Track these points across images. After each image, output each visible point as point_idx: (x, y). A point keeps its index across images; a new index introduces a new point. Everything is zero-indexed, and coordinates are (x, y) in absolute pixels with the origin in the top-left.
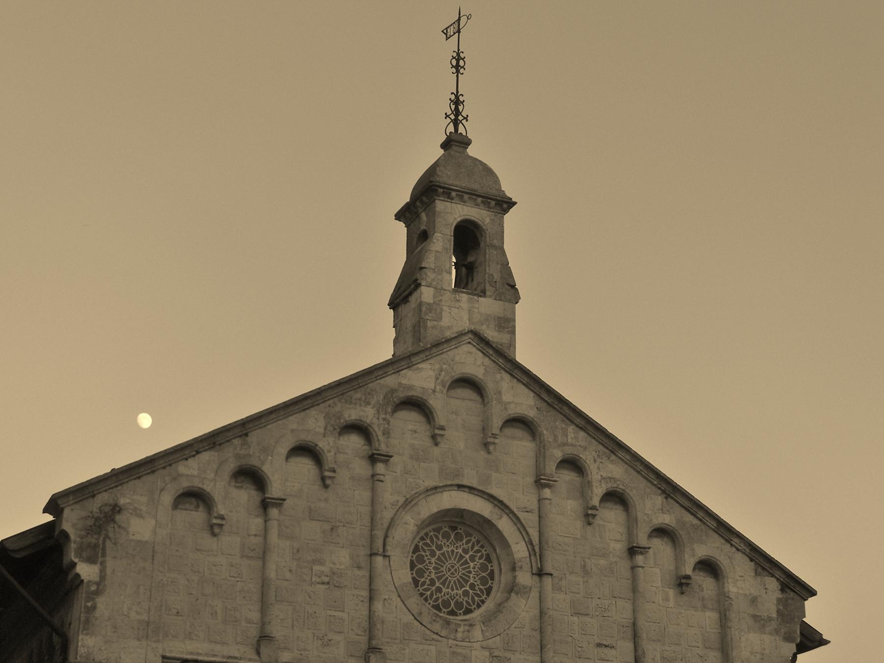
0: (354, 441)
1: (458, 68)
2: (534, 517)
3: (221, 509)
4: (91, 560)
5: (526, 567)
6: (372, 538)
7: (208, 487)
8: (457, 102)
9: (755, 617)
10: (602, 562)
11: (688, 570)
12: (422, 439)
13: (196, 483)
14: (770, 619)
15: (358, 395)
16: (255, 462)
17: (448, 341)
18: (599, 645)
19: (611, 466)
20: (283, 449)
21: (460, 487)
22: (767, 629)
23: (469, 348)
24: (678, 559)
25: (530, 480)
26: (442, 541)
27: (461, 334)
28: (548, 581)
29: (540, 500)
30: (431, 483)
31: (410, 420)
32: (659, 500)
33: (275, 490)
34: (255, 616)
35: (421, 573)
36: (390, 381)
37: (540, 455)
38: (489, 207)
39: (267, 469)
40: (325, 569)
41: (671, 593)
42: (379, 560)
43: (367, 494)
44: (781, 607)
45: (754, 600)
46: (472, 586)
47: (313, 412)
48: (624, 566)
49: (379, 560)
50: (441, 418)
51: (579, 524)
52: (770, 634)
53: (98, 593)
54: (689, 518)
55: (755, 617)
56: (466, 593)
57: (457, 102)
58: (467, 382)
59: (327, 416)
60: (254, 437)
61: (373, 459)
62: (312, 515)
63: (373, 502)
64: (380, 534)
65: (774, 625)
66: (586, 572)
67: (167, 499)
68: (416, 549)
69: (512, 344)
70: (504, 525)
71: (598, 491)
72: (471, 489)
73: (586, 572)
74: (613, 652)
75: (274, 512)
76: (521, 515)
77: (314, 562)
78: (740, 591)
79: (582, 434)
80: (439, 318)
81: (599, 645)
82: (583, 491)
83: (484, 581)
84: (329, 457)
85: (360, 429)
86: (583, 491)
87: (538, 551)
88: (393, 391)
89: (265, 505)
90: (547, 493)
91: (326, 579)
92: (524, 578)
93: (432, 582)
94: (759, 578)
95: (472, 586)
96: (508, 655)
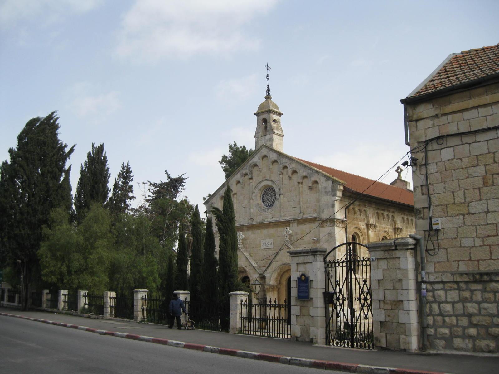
1: (268, 79)
8: (268, 87)
9: (326, 192)
10: (294, 188)
11: (310, 185)
14: (329, 192)
15: (245, 167)
18: (293, 208)
21: (265, 180)
22: (329, 194)
26: (268, 192)
27: (261, 147)
32: (303, 169)
35: (264, 200)
38: (266, 114)
40: (244, 205)
41: (309, 191)
42: (252, 201)
45: (325, 188)
46: (273, 200)
52: (329, 195)
54: (310, 172)
55: (326, 192)
57: (268, 87)
58: (265, 156)
65: (330, 193)
66: (290, 191)
71: (290, 172)
74: (296, 208)
81: (293, 208)
88: (251, 164)
93: (266, 201)
94: (327, 182)
96: (275, 214)
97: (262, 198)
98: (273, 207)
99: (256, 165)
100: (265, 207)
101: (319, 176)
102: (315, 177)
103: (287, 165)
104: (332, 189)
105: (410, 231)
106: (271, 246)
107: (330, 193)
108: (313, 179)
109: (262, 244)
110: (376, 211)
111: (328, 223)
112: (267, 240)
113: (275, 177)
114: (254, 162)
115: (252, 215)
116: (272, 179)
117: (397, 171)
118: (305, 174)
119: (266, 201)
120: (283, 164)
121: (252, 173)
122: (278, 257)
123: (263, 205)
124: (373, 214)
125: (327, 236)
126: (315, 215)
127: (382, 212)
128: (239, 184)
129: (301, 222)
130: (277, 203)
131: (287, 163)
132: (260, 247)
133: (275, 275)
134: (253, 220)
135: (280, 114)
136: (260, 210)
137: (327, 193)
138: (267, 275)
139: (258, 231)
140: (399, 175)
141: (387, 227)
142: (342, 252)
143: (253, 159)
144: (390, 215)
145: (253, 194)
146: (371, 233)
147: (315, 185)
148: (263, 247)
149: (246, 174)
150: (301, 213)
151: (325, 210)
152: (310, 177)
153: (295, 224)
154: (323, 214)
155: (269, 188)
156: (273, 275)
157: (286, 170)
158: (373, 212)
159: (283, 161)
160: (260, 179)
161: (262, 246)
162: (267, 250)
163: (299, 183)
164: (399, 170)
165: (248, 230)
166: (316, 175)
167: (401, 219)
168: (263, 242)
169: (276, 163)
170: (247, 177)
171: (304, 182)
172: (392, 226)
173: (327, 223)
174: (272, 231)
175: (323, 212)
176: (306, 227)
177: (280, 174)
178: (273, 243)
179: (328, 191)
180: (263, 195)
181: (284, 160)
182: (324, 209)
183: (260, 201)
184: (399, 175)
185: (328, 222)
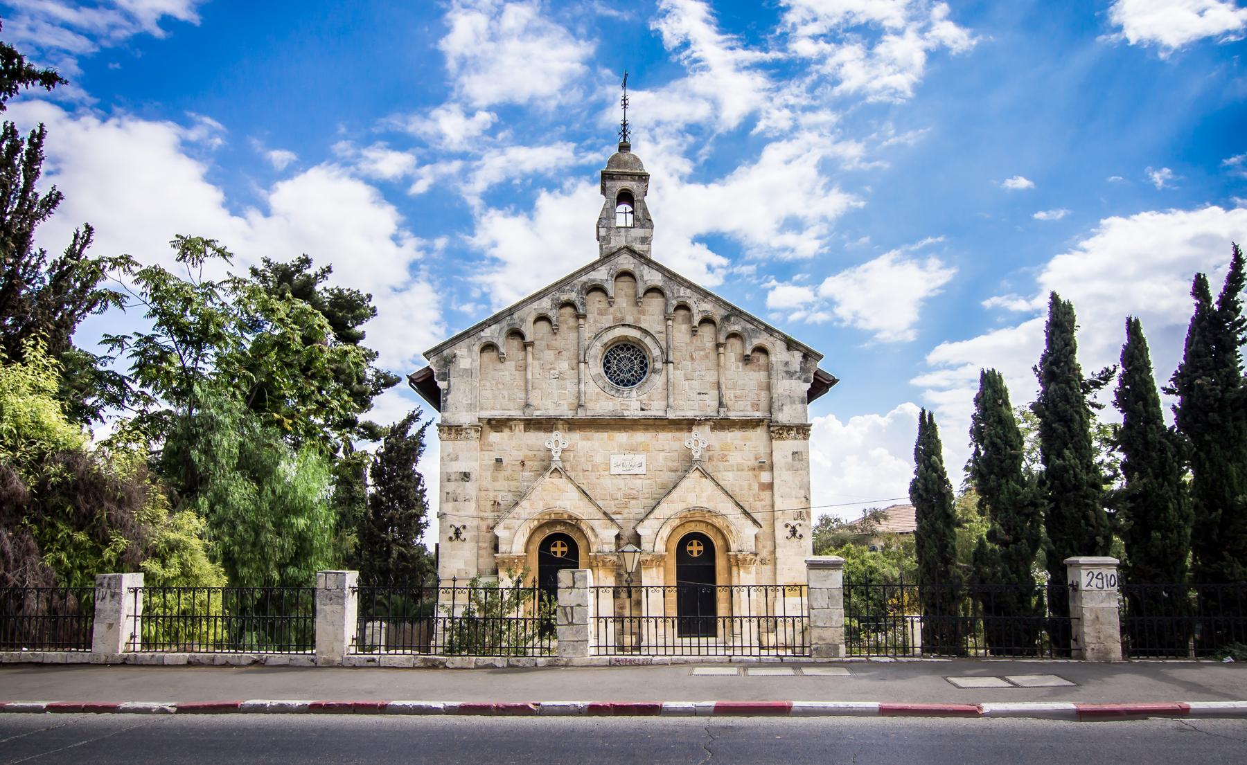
0: (568, 310)
2: (664, 335)
3: (502, 350)
4: (444, 380)
5: (660, 359)
6: (579, 355)
7: (495, 341)
10: (702, 353)
11: (748, 352)
12: (604, 305)
13: (489, 339)
14: (796, 372)
16: (517, 327)
17: (613, 254)
19: (705, 305)
20: (531, 319)
21: (623, 325)
23: (626, 256)
24: (744, 347)
25: (662, 317)
27: (620, 250)
28: (671, 365)
29: (667, 327)
30: (607, 326)
31: (596, 297)
33: (528, 339)
34: (523, 396)
36: (584, 278)
37: (666, 305)
39: (523, 329)
41: (740, 364)
42: (582, 365)
43: (576, 334)
45: (787, 364)
46: (636, 372)
47: (545, 299)
48: (713, 356)
49: (582, 365)
50: (611, 294)
51: (689, 336)
53: (447, 393)
54: (749, 326)
55: (787, 372)
56: (632, 375)
58: (626, 274)
59: (552, 300)
60: (516, 316)
61: (578, 317)
62: (549, 347)
63: (578, 338)
64: (582, 353)
66: (692, 359)
67: (477, 349)
68: (606, 357)
69: (649, 250)
70: (648, 341)
71: (697, 319)
72: (629, 326)
73: (692, 359)
75: (529, 349)
76: (657, 336)
77: (551, 369)
79: (688, 291)
80: (609, 243)
82: (690, 319)
83: (642, 368)
84: (554, 319)
85: (569, 304)
86: (690, 319)
87: (665, 352)
88: (585, 283)
89: (525, 346)
90: (670, 322)
92: (659, 365)
95: (636, 372)
101: (772, 338)
102: (763, 339)
103: (691, 302)
106: (642, 470)
111: (793, 433)
112: (630, 456)
114: (594, 280)
115: (583, 398)
120: (680, 299)
121: (583, 304)
122: (674, 494)
125: (790, 457)
126: (758, 415)
129: (722, 424)
136: (607, 389)
137: (790, 374)
139: (604, 435)
147: (757, 355)
148: (614, 471)
152: (750, 337)
153: (707, 428)
155: (625, 345)
157: (682, 312)
160: (607, 321)
163: (718, 346)
165: (570, 430)
168: (616, 459)
171: (729, 346)
174: (640, 437)
175: (781, 409)
176: (732, 437)
178: (644, 465)
179: (792, 369)
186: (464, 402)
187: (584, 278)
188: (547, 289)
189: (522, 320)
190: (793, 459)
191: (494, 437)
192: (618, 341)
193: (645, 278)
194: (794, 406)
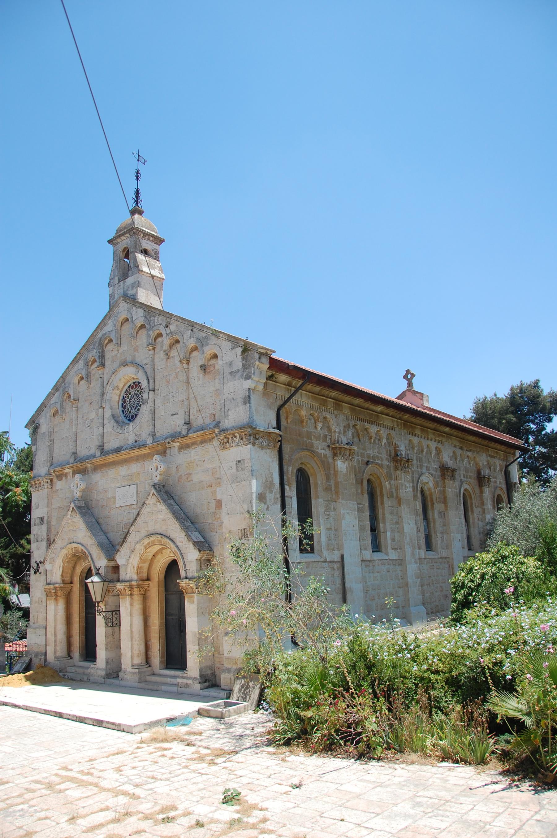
1: (137, 178)
8: (137, 193)
14: (238, 371)
15: (92, 347)
18: (172, 415)
22: (237, 377)
28: (151, 393)
35: (125, 408)
41: (201, 376)
42: (101, 410)
44: (244, 362)
45: (231, 364)
52: (238, 379)
53: (35, 455)
55: (231, 373)
57: (137, 193)
65: (240, 373)
78: (224, 362)
79: (160, 318)
81: (172, 415)
88: (101, 338)
91: (89, 424)
93: (128, 409)
97: (122, 405)
98: (137, 420)
99: (111, 341)
100: (126, 421)
101: (219, 342)
104: (243, 365)
105: (427, 467)
107: (240, 373)
108: (209, 350)
109: (117, 498)
110: (352, 423)
113: (143, 356)
116: (138, 360)
117: (405, 377)
118: (192, 343)
119: (128, 409)
121: (102, 356)
123: (122, 418)
124: (347, 427)
127: (367, 425)
128: (82, 382)
130: (145, 410)
131: (160, 324)
132: (114, 503)
133: (135, 561)
134: (103, 449)
135: (159, 241)
138: (120, 559)
140: (410, 384)
141: (378, 457)
142: (268, 503)
143: (105, 328)
144: (384, 433)
145: (104, 398)
146: (341, 465)
147: (213, 362)
148: (119, 503)
149: (94, 361)
150: (185, 424)
151: (230, 412)
154: (226, 421)
155: (134, 383)
156: (131, 560)
157: (160, 340)
158: (346, 423)
159: (154, 322)
161: (117, 501)
162: (125, 508)
163: (181, 362)
164: (409, 376)
166: (213, 339)
167: (407, 442)
169: (143, 330)
170: (95, 365)
171: (191, 361)
172: (390, 455)
173: (235, 438)
177: (149, 350)
179: (235, 369)
180: (124, 398)
181: (156, 321)
182: (228, 411)
183: (119, 411)
184: (410, 384)
185: (235, 437)
186: (43, 460)
187: (100, 335)
188: (79, 353)
189: (69, 384)
190: (237, 470)
191: (59, 485)
192: (128, 381)
193: (134, 319)
194: (237, 409)
